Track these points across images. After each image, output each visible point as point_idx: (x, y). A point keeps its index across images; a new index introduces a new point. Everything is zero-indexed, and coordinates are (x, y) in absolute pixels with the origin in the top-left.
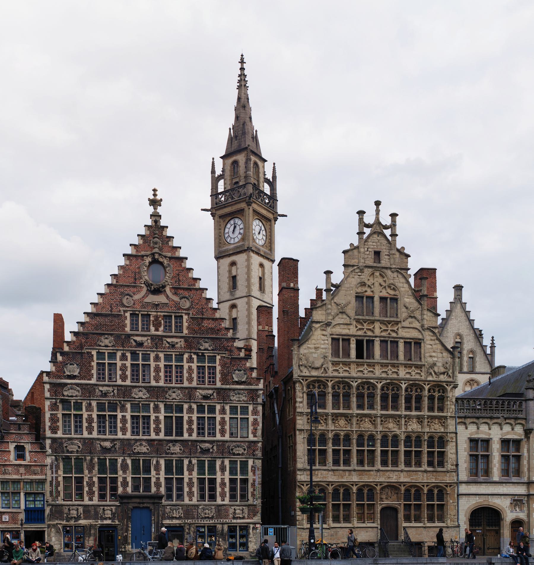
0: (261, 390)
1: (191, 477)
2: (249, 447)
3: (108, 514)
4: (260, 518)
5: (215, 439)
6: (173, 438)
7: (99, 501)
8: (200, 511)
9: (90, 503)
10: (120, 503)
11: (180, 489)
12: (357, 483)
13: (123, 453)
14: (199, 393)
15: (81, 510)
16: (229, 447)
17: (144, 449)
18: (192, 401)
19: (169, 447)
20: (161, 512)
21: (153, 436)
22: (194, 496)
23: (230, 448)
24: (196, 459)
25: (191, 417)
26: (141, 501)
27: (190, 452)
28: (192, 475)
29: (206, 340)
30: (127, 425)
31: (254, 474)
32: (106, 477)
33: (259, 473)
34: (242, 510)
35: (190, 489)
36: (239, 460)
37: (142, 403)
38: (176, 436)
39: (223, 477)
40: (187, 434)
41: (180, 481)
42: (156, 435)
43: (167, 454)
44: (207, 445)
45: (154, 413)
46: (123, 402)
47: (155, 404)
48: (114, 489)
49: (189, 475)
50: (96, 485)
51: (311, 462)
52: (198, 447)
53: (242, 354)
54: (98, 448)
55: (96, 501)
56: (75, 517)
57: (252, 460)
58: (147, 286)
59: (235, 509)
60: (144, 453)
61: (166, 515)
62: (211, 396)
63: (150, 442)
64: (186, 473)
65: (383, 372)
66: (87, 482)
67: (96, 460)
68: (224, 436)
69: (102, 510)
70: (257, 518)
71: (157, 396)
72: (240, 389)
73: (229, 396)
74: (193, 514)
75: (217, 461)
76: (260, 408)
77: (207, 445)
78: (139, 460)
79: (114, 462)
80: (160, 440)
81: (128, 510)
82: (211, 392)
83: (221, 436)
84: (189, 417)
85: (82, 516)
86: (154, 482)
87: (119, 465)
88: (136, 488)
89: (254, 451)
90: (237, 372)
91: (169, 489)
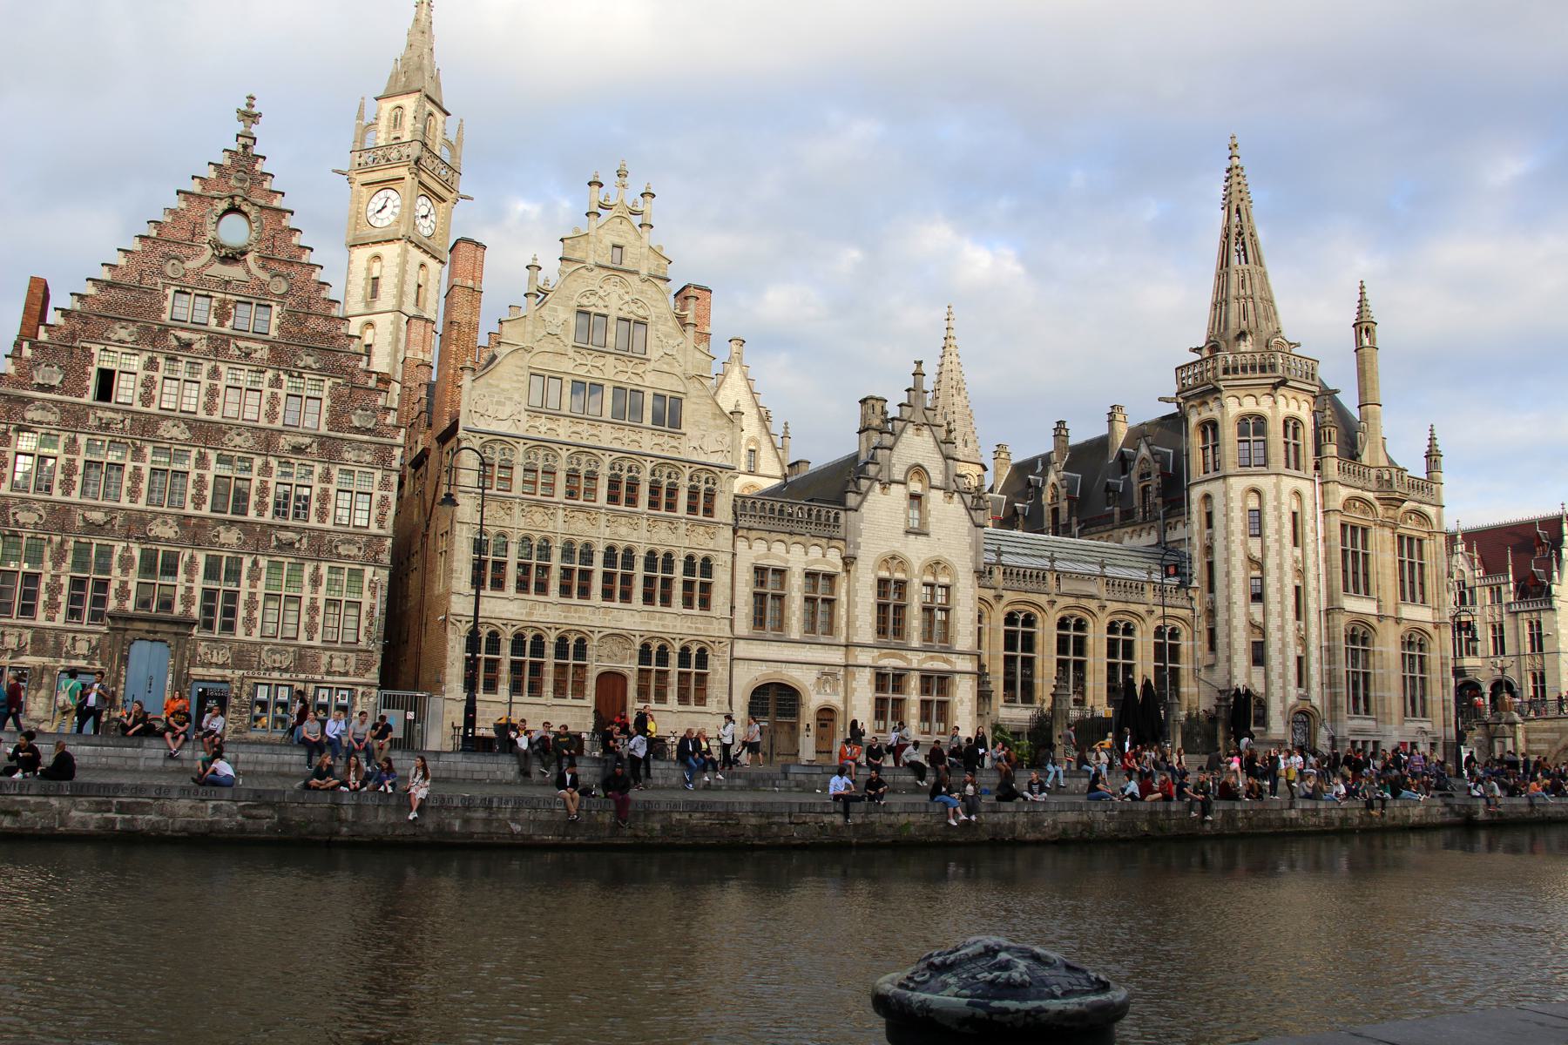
0: (399, 446)
1: (253, 590)
2: (368, 545)
3: (82, 647)
4: (377, 676)
5: (306, 525)
6: (229, 516)
7: (66, 622)
8: (264, 655)
9: (49, 624)
10: (111, 629)
11: (230, 612)
12: (558, 626)
13: (128, 537)
14: (285, 442)
15: (28, 635)
16: (331, 542)
17: (169, 532)
18: (272, 453)
19: (218, 532)
20: (188, 653)
21: (190, 509)
22: (255, 627)
23: (333, 544)
24: (267, 558)
25: (267, 482)
26: (152, 629)
27: (258, 544)
28: (255, 587)
29: (310, 351)
30: (141, 485)
31: (374, 595)
32: (88, 578)
33: (382, 593)
34: (346, 659)
35: (250, 613)
36: (347, 566)
37: (176, 447)
38: (233, 513)
39: (314, 596)
40: (255, 512)
41: (232, 597)
42: (196, 509)
43: (212, 543)
44: (290, 535)
45: (196, 467)
46: (138, 442)
47: (200, 452)
48: (100, 601)
49: (251, 586)
50: (65, 591)
51: (478, 582)
52: (273, 536)
53: (372, 383)
54: (79, 522)
55: (60, 620)
56: (12, 650)
57: (373, 568)
58: (213, 249)
59: (331, 657)
60: (168, 540)
61: (198, 658)
62: (307, 447)
63: (183, 521)
64: (245, 582)
65: (616, 438)
66: (47, 584)
67: (71, 544)
68: (324, 522)
69: (69, 642)
70: (373, 676)
71: (207, 439)
72: (361, 442)
73: (339, 452)
74: (249, 661)
75: (306, 566)
76: (395, 478)
77: (290, 535)
78: (157, 550)
79: (106, 552)
80: (202, 518)
81: (124, 644)
82: (308, 440)
83: (319, 522)
84: (262, 482)
85: (28, 647)
86: (182, 596)
87: (116, 558)
88: (144, 603)
89: (377, 553)
90: (359, 411)
91: (208, 610)
